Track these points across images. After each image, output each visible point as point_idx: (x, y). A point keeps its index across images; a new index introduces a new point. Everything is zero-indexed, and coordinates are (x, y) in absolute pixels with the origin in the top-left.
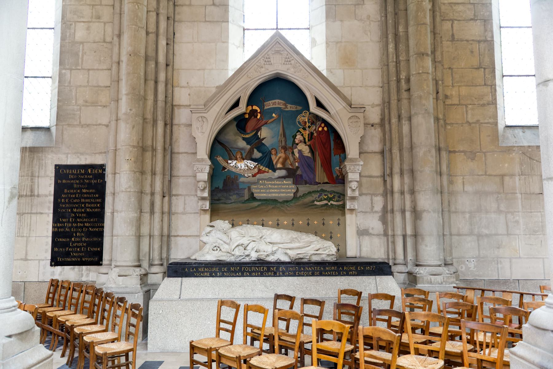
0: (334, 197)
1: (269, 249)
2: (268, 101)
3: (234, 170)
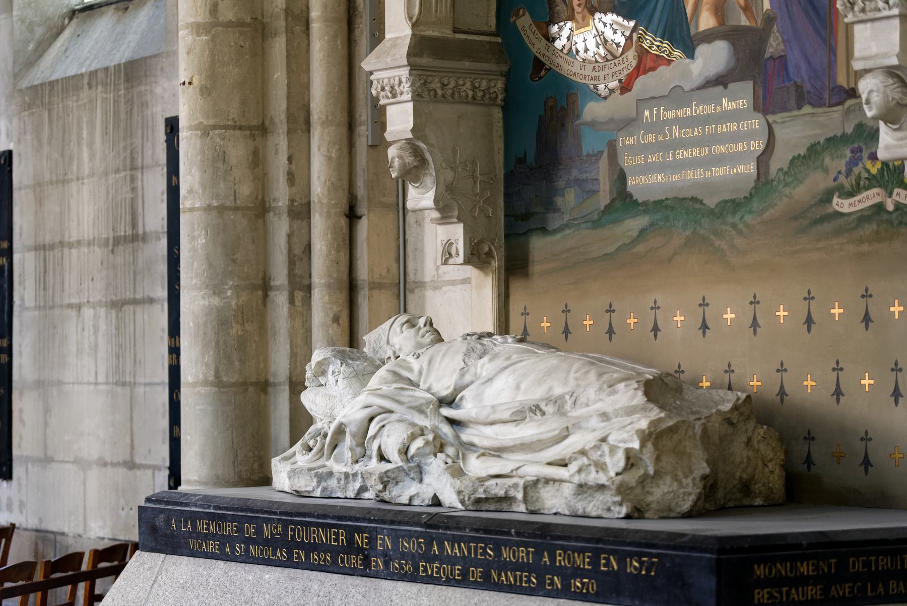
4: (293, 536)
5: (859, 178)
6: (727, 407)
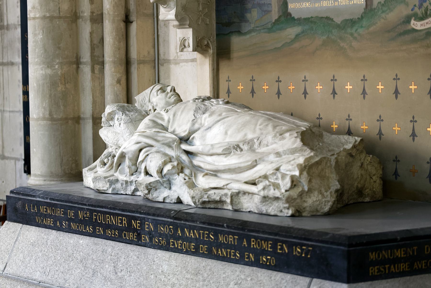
4: (96, 219)
5: (427, 9)
6: (349, 146)
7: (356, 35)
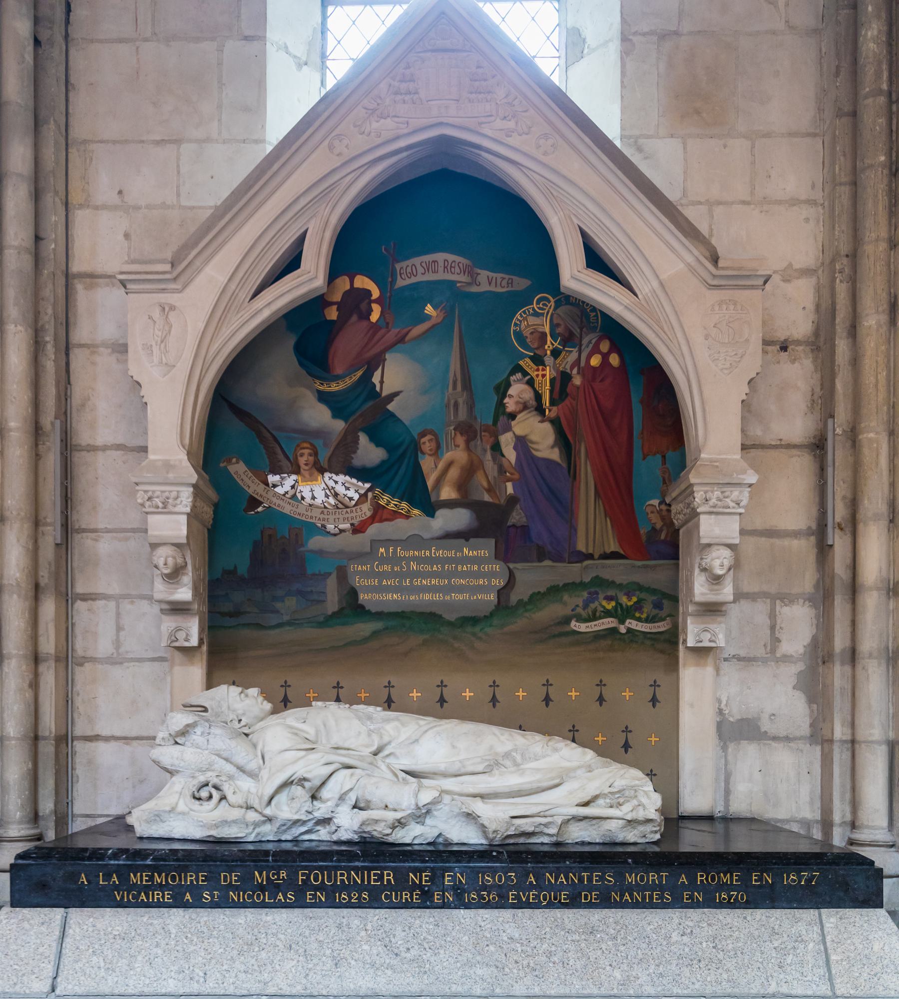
0: (638, 607)
1: (406, 797)
2: (407, 258)
3: (287, 509)
5: (595, 611)
7: (480, 635)
